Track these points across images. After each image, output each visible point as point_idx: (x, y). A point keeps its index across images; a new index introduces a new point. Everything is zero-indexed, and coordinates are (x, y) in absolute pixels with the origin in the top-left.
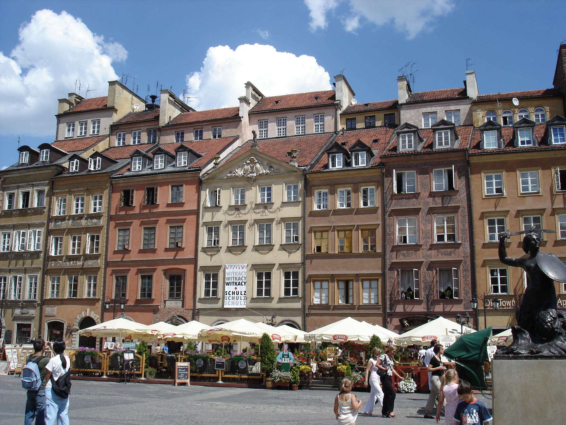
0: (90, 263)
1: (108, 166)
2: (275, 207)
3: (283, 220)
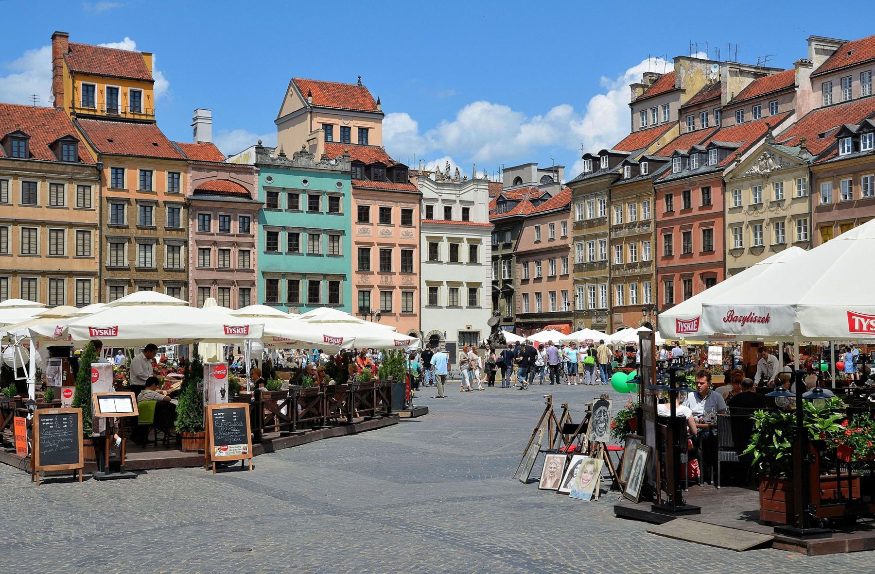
0: (645, 270)
1: (657, 169)
2: (786, 203)
3: (794, 217)
